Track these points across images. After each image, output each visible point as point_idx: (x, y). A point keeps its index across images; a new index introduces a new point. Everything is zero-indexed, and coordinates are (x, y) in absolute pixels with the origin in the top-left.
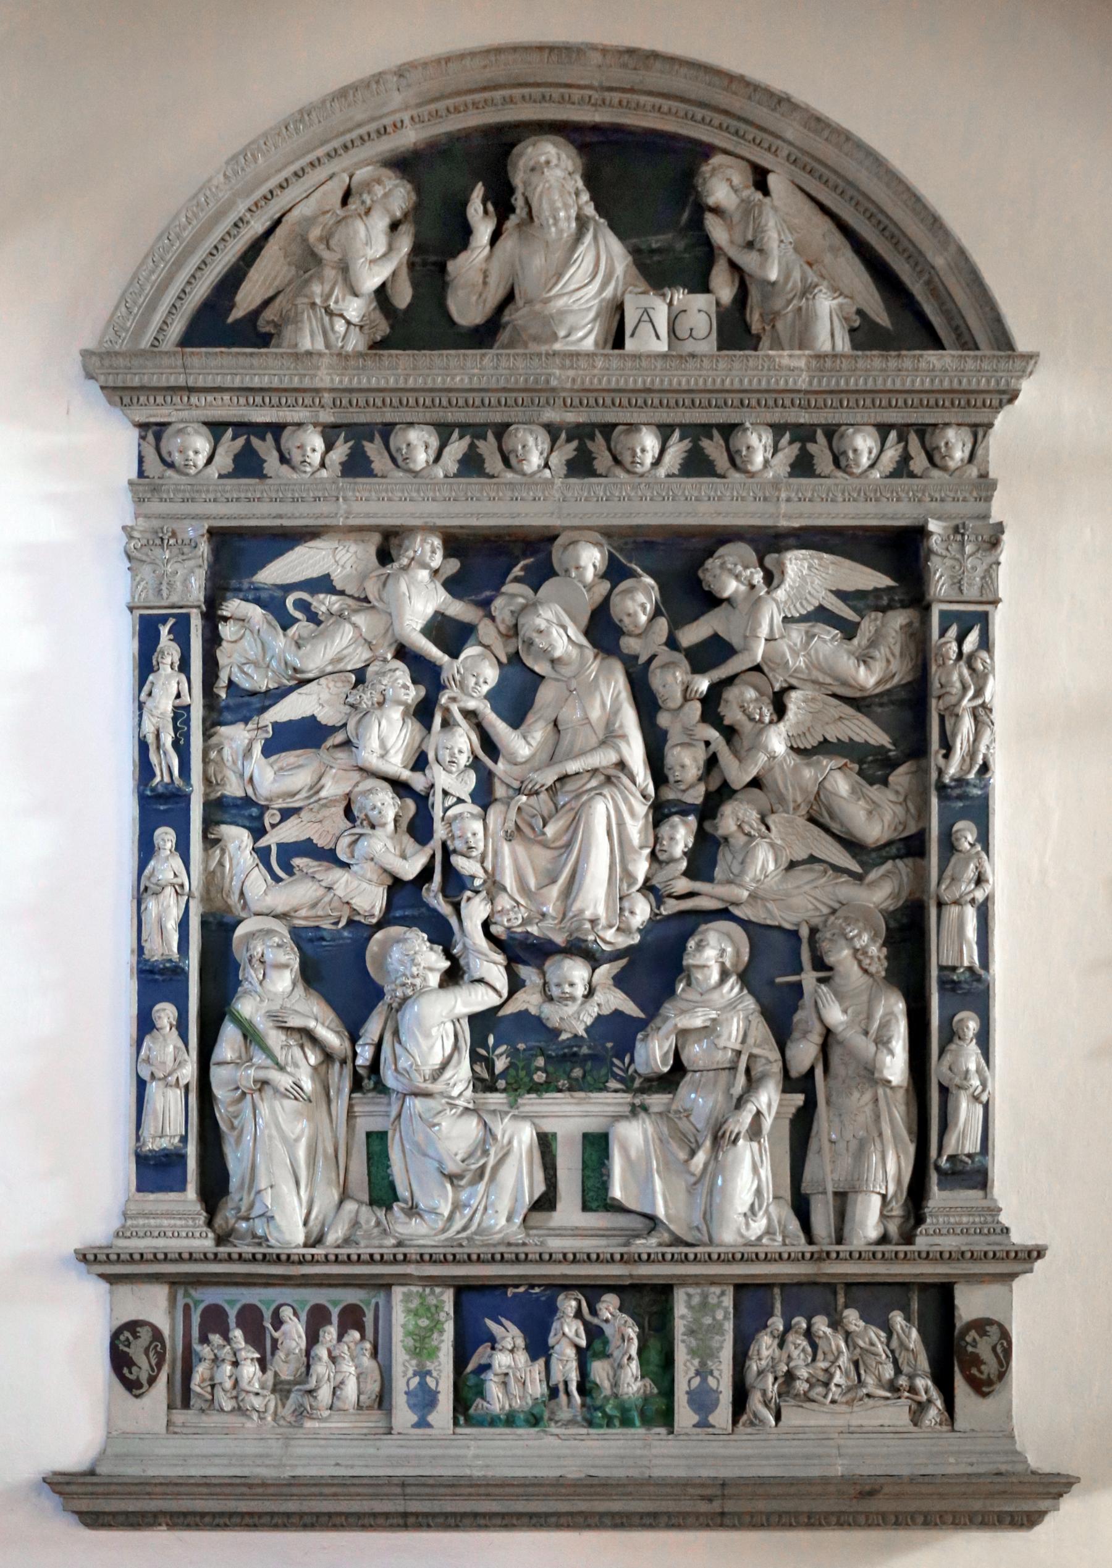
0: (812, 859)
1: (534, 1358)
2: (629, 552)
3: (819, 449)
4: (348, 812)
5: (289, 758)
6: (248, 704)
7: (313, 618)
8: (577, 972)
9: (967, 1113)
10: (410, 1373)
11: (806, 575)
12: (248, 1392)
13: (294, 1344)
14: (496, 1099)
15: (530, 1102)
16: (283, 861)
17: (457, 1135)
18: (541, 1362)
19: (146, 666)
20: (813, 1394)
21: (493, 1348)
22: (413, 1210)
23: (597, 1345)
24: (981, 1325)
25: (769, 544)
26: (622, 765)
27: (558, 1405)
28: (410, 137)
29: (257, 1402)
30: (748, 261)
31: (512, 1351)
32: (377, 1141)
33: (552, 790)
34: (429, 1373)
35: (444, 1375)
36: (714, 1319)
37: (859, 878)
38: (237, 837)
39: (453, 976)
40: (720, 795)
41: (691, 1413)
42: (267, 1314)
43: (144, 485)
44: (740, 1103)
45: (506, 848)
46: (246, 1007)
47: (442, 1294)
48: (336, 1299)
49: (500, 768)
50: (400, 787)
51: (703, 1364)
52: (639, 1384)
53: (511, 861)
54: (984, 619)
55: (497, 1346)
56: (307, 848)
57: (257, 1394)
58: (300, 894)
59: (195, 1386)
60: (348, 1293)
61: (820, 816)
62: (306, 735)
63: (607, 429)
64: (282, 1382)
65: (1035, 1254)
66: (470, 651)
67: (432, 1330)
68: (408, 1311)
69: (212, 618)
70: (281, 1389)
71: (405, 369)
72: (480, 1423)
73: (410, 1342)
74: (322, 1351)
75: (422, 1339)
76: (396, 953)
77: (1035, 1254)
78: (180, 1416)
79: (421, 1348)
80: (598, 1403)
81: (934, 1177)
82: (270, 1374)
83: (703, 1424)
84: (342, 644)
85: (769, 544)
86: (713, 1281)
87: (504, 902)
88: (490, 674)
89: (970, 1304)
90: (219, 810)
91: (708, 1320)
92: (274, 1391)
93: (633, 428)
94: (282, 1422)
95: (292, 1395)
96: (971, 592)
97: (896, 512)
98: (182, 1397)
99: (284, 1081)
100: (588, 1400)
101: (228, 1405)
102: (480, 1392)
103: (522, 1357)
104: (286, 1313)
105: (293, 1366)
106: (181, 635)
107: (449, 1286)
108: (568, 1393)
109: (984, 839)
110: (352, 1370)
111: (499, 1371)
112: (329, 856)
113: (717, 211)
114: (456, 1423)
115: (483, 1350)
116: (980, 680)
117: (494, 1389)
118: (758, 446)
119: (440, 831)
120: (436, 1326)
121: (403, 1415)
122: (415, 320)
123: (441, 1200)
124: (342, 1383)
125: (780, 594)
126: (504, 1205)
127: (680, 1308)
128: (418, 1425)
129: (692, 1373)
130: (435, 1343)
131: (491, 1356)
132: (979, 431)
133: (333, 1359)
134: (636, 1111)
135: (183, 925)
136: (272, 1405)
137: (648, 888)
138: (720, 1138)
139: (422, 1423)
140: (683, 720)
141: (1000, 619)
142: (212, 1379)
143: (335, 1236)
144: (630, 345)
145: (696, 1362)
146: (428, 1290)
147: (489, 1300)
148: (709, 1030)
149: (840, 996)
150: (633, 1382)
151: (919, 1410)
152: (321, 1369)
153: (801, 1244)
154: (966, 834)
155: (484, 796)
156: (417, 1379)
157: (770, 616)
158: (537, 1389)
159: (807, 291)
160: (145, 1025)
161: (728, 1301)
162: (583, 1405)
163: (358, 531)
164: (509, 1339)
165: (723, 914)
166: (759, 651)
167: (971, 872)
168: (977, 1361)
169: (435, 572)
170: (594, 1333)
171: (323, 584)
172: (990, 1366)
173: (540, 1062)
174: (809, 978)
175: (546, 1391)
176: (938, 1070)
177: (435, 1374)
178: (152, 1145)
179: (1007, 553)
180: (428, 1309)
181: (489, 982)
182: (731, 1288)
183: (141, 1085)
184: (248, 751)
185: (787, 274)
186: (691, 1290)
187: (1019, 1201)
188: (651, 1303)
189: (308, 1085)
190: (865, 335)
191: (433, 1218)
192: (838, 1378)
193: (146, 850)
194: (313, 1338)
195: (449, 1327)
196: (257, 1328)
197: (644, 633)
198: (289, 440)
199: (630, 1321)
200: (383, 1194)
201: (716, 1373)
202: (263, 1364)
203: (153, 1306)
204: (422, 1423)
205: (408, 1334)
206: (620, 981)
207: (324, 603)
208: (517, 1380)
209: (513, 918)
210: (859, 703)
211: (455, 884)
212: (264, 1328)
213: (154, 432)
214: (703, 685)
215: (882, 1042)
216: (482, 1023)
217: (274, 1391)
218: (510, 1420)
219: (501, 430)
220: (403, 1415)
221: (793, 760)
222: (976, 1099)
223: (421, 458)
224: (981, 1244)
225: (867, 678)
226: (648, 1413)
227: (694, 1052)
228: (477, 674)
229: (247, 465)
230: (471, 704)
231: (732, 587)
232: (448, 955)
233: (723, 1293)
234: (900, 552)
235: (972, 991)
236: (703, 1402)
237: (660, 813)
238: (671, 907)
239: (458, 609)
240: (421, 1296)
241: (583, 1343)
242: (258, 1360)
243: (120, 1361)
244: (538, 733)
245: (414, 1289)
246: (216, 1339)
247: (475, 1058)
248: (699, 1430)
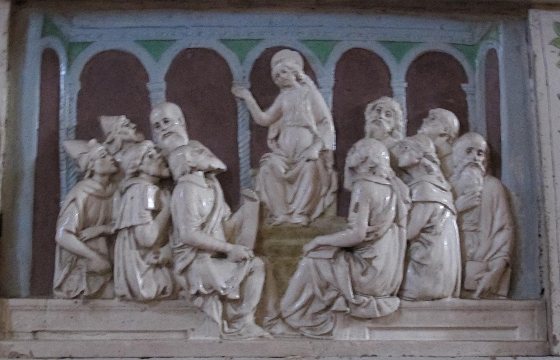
12: (200, 249)
13: (307, 138)
29: (223, 275)
42: (240, 70)
57: (221, 255)
59: (66, 232)
64: (278, 230)
70: (276, 247)
74: (375, 150)
82: (249, 209)
92: (258, 251)
94: (279, 329)
95: (305, 263)
101: (148, 284)
104: (287, 64)
105: (303, 191)
110: (447, 199)
124: (428, 228)
133: (401, 171)
136: (257, 283)
142: (107, 221)
152: (377, 192)
194: (350, 128)
202: (230, 185)
212: (232, 102)
217: (258, 251)
242: (221, 176)
246: (117, 125)
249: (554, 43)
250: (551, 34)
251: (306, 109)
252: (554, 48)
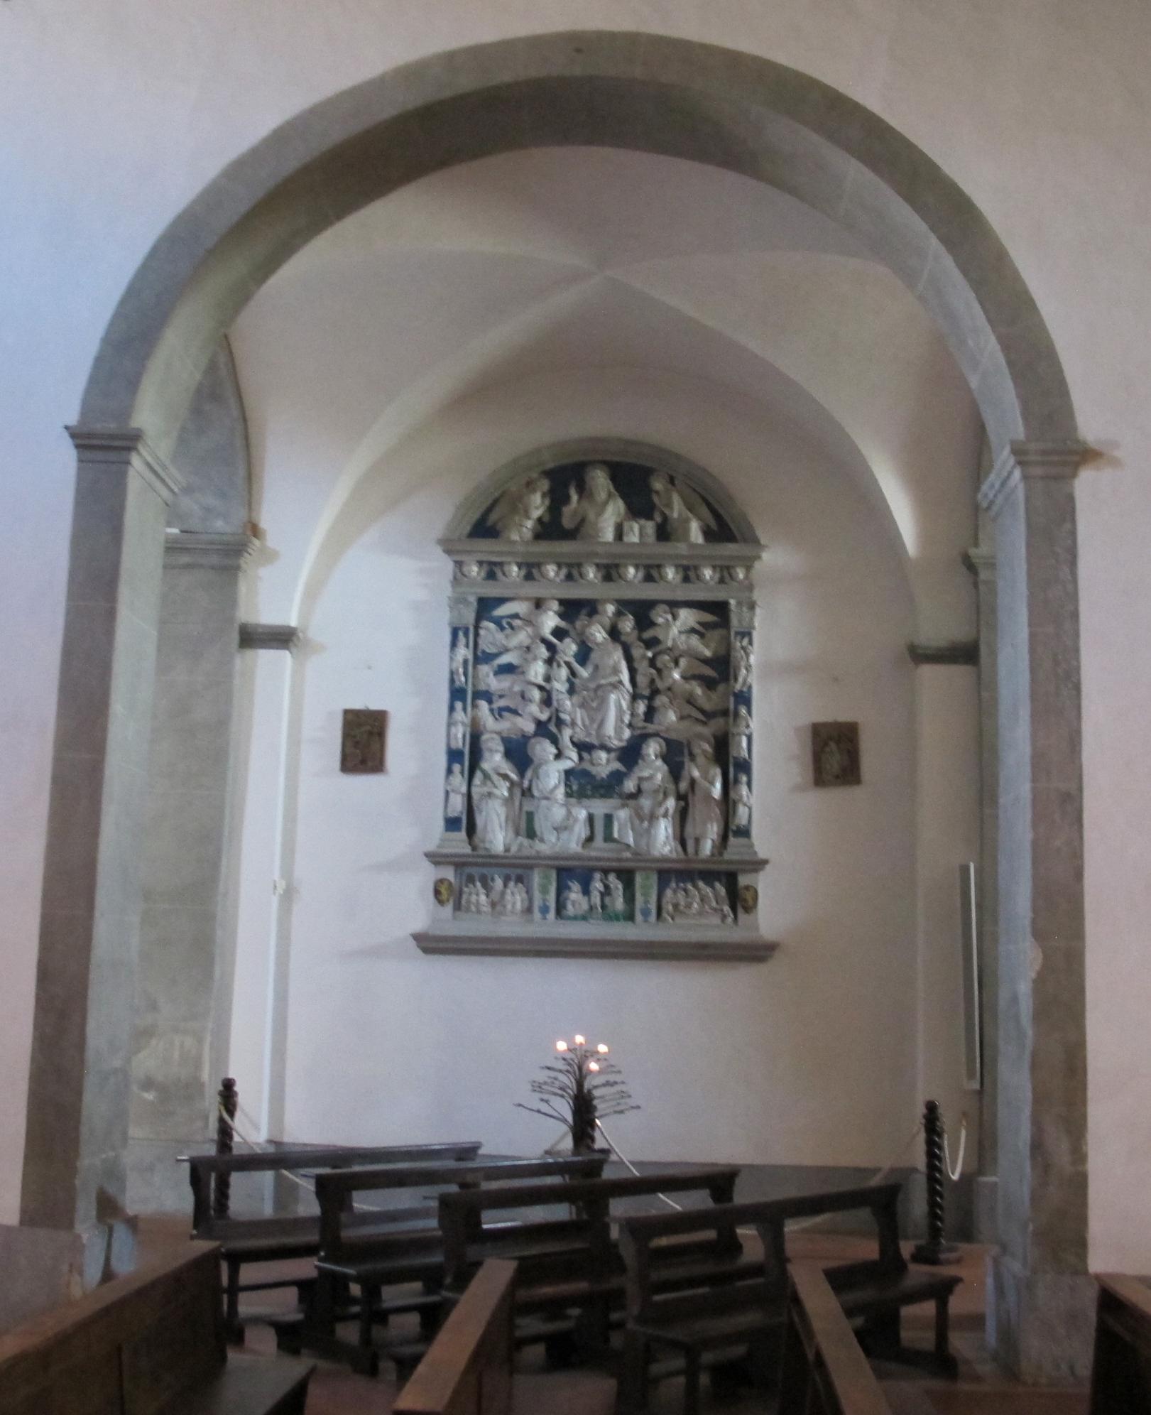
0: (689, 716)
2: (625, 606)
3: (692, 574)
4: (523, 697)
5: (502, 677)
6: (487, 658)
7: (512, 628)
8: (603, 755)
9: (742, 811)
11: (687, 617)
14: (573, 800)
15: (586, 802)
16: (499, 713)
17: (558, 813)
19: (454, 644)
20: (687, 911)
22: (542, 840)
24: (747, 888)
25: (674, 605)
26: (621, 682)
28: (551, 465)
30: (667, 512)
32: (530, 816)
33: (596, 690)
37: (704, 723)
38: (483, 704)
39: (559, 756)
40: (655, 692)
43: (456, 581)
44: (660, 804)
45: (578, 711)
46: (485, 765)
48: (513, 872)
49: (577, 681)
50: (541, 688)
53: (579, 715)
54: (749, 634)
56: (508, 709)
58: (505, 725)
59: (463, 902)
60: (517, 870)
61: (690, 701)
62: (508, 669)
63: (617, 566)
65: (765, 862)
66: (567, 640)
69: (477, 627)
70: (493, 905)
71: (545, 547)
74: (508, 891)
76: (538, 747)
77: (765, 862)
78: (458, 913)
79: (544, 891)
81: (731, 835)
84: (522, 637)
85: (674, 605)
86: (651, 869)
87: (578, 730)
88: (574, 647)
89: (743, 880)
90: (478, 695)
93: (626, 566)
96: (745, 624)
97: (719, 595)
98: (458, 907)
99: (496, 792)
102: (565, 907)
103: (580, 896)
104: (496, 877)
106: (466, 635)
109: (749, 712)
112: (515, 712)
113: (657, 492)
116: (747, 655)
117: (570, 907)
118: (670, 573)
119: (555, 703)
121: (537, 915)
122: (550, 529)
123: (551, 837)
125: (678, 623)
126: (574, 838)
127: (639, 879)
132: (748, 568)
134: (623, 806)
135: (464, 736)
137: (630, 726)
138: (653, 818)
140: (643, 667)
141: (755, 635)
143: (514, 849)
144: (626, 539)
147: (570, 873)
148: (650, 778)
149: (698, 767)
150: (619, 903)
151: (724, 917)
152: (508, 897)
153: (682, 856)
154: (743, 711)
155: (572, 691)
157: (674, 631)
158: (585, 907)
159: (687, 521)
160: (449, 771)
163: (527, 599)
165: (656, 735)
166: (670, 644)
167: (744, 723)
168: (745, 900)
169: (556, 613)
170: (607, 887)
171: (516, 616)
172: (751, 902)
173: (589, 787)
174: (686, 759)
176: (732, 795)
178: (451, 814)
179: (758, 611)
181: (572, 758)
183: (447, 793)
184: (488, 675)
185: (680, 514)
187: (762, 842)
188: (627, 877)
189: (506, 794)
190: (709, 535)
191: (549, 843)
192: (695, 905)
193: (452, 709)
194: (505, 886)
196: (486, 883)
197: (628, 634)
198: (506, 568)
200: (531, 834)
202: (487, 896)
203: (449, 874)
204: (545, 918)
206: (620, 759)
207: (517, 622)
209: (581, 736)
210: (706, 661)
211: (560, 723)
213: (459, 564)
214: (650, 654)
215: (712, 783)
216: (568, 773)
218: (575, 918)
219: (579, 565)
220: (537, 915)
221: (682, 681)
222: (745, 805)
223: (552, 574)
224: (747, 858)
225: (708, 653)
227: (645, 786)
228: (569, 648)
229: (491, 576)
230: (567, 659)
231: (660, 620)
232: (557, 748)
234: (719, 609)
235: (744, 766)
236: (646, 913)
237: (635, 697)
238: (639, 732)
239: (563, 624)
243: (437, 893)
244: (590, 668)
247: (566, 785)
251: (499, 883)
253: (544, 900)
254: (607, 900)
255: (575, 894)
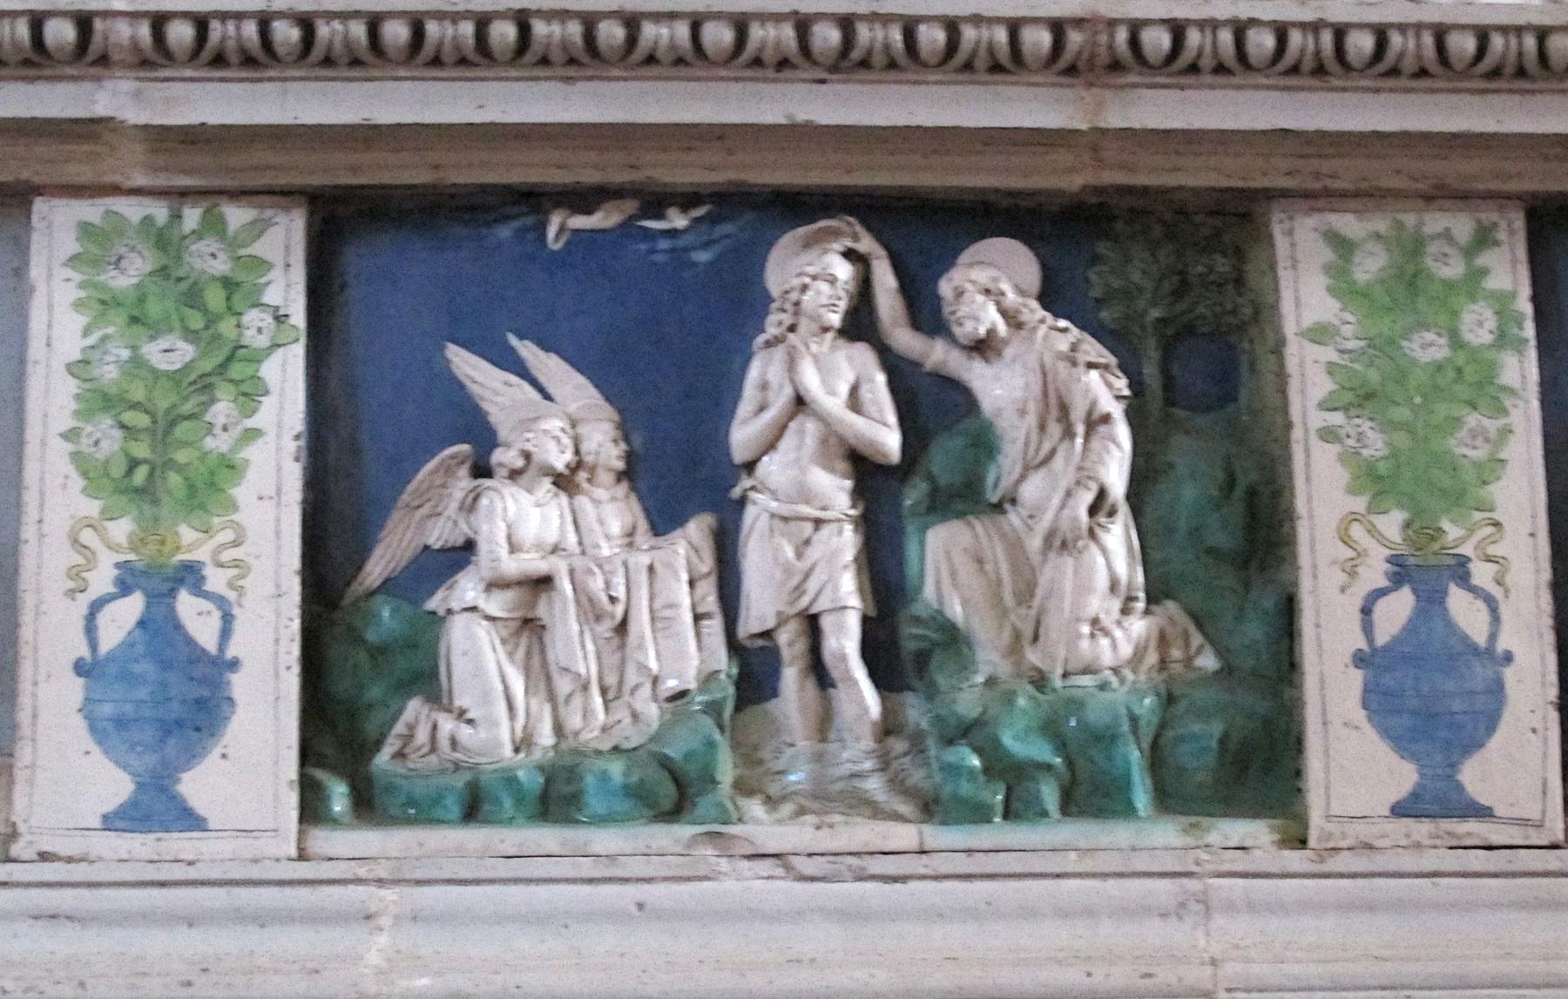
1: (663, 520)
10: (102, 579)
18: (697, 530)
21: (482, 470)
23: (943, 458)
27: (774, 728)
31: (564, 482)
34: (190, 575)
35: (258, 585)
36: (1457, 343)
41: (1383, 752)
47: (258, 229)
51: (1422, 531)
52: (1139, 626)
55: (505, 457)
67: (205, 387)
68: (103, 304)
72: (422, 813)
73: (106, 439)
75: (165, 428)
79: (159, 468)
80: (967, 702)
83: (1437, 801)
91: (1427, 348)
100: (915, 710)
102: (424, 677)
103: (611, 512)
107: (284, 195)
108: (819, 671)
111: (512, 566)
114: (312, 810)
115: (441, 473)
117: (477, 651)
120: (229, 369)
128: (125, 819)
129: (1375, 574)
130: (218, 443)
131: (470, 506)
139: (156, 807)
145: (1392, 524)
146: (192, 216)
156: (132, 607)
158: (686, 655)
161: (1508, 273)
162: (888, 728)
164: (555, 424)
170: (930, 403)
175: (721, 659)
177: (216, 580)
180: (193, 297)
182: (1519, 222)
186: (1347, 223)
195: (286, 375)
199: (1093, 349)
201: (1482, 574)
204: (156, 807)
205: (98, 401)
208: (591, 611)
226: (1185, 756)
233: (1484, 238)
240: (164, 241)
241: (889, 441)
245: (132, 210)
248: (1421, 829)
249: (73, 261)
250: (69, 244)
252: (70, 273)
253: (161, 581)
254: (945, 562)
255: (541, 497)
